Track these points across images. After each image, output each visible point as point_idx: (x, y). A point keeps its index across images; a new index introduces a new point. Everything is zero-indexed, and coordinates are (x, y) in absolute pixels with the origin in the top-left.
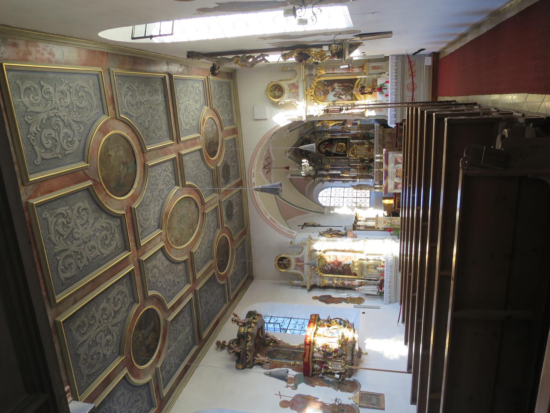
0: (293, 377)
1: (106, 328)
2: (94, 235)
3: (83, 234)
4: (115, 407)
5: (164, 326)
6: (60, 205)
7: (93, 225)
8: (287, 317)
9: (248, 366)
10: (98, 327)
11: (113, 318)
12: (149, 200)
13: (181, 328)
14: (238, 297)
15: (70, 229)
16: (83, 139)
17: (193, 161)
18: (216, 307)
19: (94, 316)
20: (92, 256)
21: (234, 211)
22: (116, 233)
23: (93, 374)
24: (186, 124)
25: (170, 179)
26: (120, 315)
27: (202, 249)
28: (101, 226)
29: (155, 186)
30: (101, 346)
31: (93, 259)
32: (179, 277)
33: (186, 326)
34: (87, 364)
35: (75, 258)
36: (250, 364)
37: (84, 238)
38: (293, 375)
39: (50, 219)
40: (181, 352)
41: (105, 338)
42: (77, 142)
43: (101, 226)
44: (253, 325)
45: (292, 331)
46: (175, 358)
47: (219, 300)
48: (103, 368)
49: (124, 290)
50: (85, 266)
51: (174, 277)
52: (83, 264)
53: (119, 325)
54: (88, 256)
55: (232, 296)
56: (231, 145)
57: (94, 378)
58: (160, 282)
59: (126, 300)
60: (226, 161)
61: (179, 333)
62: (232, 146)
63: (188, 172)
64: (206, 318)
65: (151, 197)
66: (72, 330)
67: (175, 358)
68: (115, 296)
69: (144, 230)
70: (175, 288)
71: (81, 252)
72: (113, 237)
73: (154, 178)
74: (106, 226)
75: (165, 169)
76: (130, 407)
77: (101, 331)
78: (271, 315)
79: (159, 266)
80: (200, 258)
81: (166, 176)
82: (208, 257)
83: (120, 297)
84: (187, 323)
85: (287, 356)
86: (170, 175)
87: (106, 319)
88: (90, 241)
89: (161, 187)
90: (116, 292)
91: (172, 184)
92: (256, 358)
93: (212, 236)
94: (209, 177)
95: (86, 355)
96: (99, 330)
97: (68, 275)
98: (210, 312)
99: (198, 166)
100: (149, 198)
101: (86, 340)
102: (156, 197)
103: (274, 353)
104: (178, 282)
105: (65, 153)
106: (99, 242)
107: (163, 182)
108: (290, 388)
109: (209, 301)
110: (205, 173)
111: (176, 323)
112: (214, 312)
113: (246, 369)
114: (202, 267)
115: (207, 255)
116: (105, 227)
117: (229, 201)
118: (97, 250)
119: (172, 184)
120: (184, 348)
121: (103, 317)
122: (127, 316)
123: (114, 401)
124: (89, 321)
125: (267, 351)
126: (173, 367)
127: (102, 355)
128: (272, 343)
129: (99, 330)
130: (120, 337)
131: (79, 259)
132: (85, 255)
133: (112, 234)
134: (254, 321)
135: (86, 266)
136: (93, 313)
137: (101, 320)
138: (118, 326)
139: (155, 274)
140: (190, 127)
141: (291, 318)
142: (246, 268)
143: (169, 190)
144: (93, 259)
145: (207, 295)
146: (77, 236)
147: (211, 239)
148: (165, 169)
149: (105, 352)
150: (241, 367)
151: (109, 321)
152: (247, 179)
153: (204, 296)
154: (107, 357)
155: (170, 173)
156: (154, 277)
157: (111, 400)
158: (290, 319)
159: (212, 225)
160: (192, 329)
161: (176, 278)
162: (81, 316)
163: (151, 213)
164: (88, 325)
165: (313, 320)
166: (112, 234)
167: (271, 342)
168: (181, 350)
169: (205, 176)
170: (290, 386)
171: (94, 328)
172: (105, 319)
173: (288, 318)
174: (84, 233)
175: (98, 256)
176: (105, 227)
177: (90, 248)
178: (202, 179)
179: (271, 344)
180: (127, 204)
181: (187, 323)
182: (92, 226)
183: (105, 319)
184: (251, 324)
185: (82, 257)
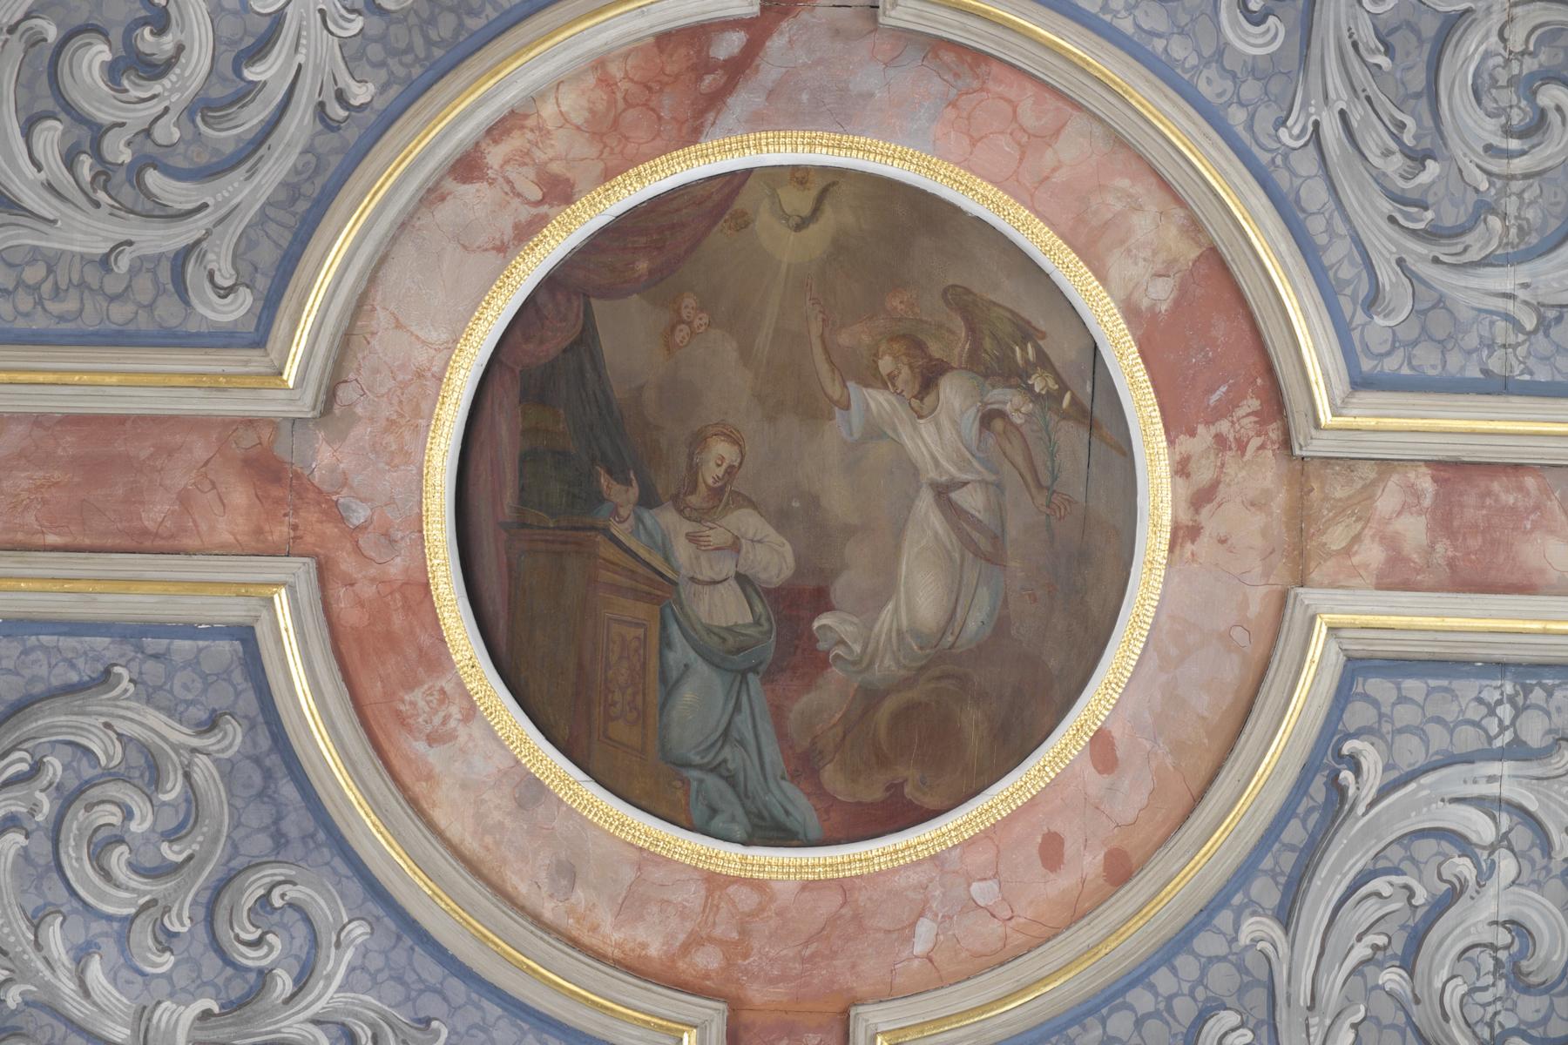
12: (264, 975)
22: (119, 232)
72: (105, 173)
74: (253, 88)
100: (284, 983)
116: (251, 74)
133: (136, 172)
166: (136, 172)
176: (251, 74)
180: (360, 515)
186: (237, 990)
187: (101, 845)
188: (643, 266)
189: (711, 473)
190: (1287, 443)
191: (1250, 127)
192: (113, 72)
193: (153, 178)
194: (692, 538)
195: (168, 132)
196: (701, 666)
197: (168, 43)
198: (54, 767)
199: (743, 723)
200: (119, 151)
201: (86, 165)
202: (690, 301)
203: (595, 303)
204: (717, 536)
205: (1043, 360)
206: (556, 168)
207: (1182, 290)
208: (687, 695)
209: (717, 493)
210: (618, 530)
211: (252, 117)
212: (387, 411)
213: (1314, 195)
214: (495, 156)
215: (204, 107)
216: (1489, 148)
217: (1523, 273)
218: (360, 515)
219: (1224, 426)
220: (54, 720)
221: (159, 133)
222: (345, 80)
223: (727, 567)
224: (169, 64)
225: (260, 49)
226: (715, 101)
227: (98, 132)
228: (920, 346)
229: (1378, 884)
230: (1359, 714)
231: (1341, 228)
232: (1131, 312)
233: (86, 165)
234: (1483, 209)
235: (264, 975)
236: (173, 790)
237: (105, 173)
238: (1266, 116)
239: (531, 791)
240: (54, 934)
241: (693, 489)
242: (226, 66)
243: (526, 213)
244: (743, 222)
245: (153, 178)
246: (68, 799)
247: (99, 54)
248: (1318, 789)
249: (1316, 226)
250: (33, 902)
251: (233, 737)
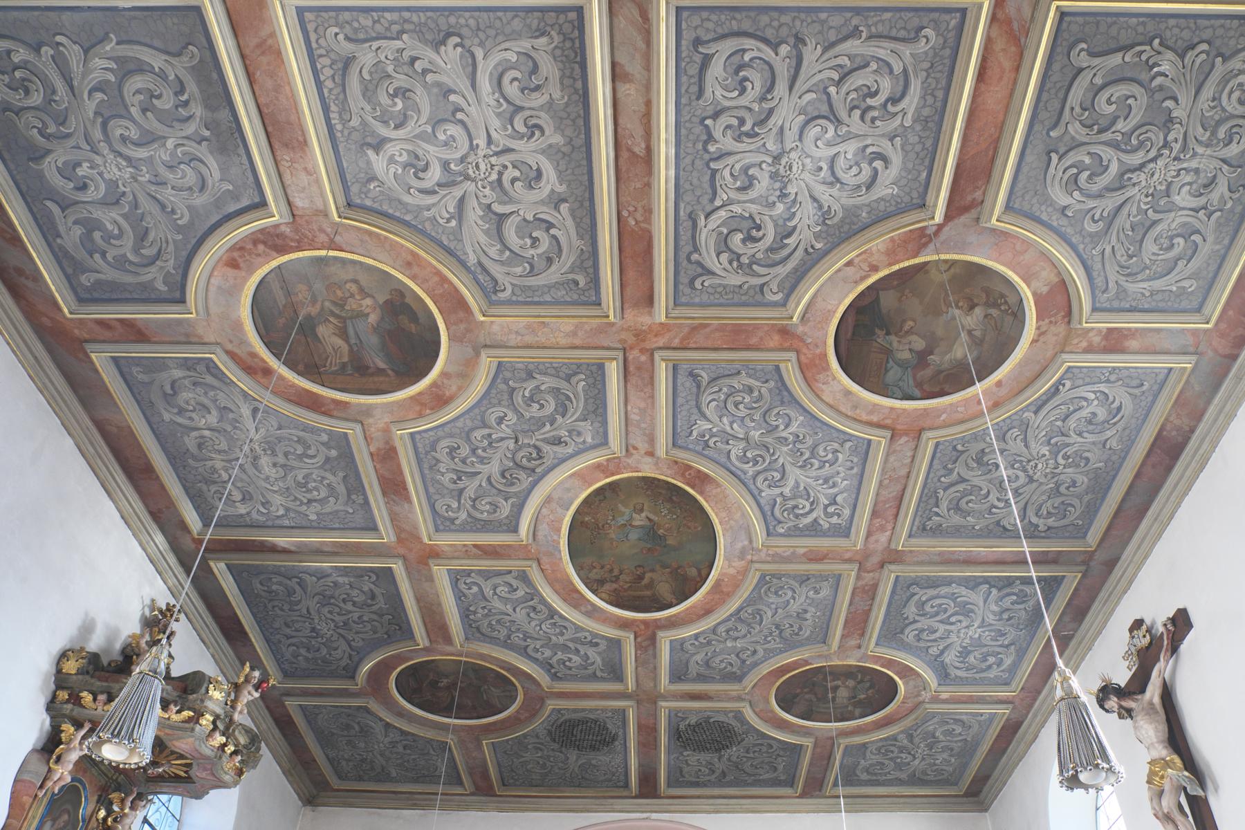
1: (470, 172)
2: (783, 196)
3: (808, 156)
4: (170, 143)
5: (345, 405)
6: (928, 97)
7: (815, 199)
9: (63, 695)
10: (490, 141)
11: (489, 206)
12: (777, 427)
13: (300, 478)
14: (276, 732)
15: (843, 114)
16: (1064, 222)
17: (806, 611)
18: (288, 637)
19: (537, 133)
20: (726, 173)
21: (573, 755)
23: (344, 86)
24: (924, 603)
25: (797, 516)
26: (483, 239)
27: (518, 610)
28: (795, 228)
29: (807, 455)
30: (422, 136)
31: (714, 172)
32: (474, 501)
33: (296, 499)
34: (390, 69)
35: (750, 109)
36: (68, 701)
37: (793, 155)
39: (906, 51)
40: (209, 463)
41: (439, 159)
42: (1063, 199)
43: (795, 228)
44: (219, 739)
46: (207, 433)
47: (308, 650)
48: (339, 127)
49: (553, 268)
50: (710, 138)
51: (489, 479)
52: (717, 134)
53: (453, 223)
54: (730, 160)
55: (291, 704)
56: (781, 767)
57: (329, 84)
58: (500, 420)
59: (518, 270)
60: (743, 740)
61: (283, 466)
62: (776, 769)
63: (782, 588)
64: (274, 587)
65: (784, 434)
66: (536, 37)
67: (207, 433)
68: (553, 231)
69: (699, 387)
70: (446, 479)
71: (757, 135)
72: (740, 266)
73: (830, 456)
74: (786, 245)
75: (835, 503)
76: (136, 205)
77: (473, 148)
79: (555, 426)
80: (495, 593)
81: (812, 504)
82: (478, 628)
83: (540, 251)
84: (302, 503)
86: (808, 520)
87: (499, 180)
88: (774, 176)
89: (794, 474)
90: (563, 240)
91: (780, 522)
93: (538, 656)
94: (729, 668)
95: (425, 72)
96: (481, 141)
97: (717, 69)
98: (286, 607)
99: (780, 633)
100: (782, 427)
101: (474, 85)
102: (773, 454)
103: (66, 817)
104: (461, 491)
105: (1057, 152)
106: (754, 208)
107: (802, 488)
109: (325, 610)
110: (744, 657)
111: (328, 460)
112: (277, 625)
113: (53, 687)
114: (459, 596)
115: (490, 625)
116: (785, 241)
117: (614, 739)
118: (733, 195)
119: (780, 522)
120: (220, 476)
121: (514, 167)
122: (463, 264)
123: (199, 143)
124: (528, 113)
125: (84, 788)
126: (180, 420)
127: (384, 131)
128: (105, 819)
129: (481, 141)
130: (408, 218)
131: (742, 122)
132: (741, 147)
134: (230, 749)
135: (706, 143)
136: (547, 133)
137: (506, 159)
138: (448, 221)
139: (538, 402)
140: (907, 618)
142: (360, 779)
143: (767, 508)
144: (714, 172)
145: (354, 604)
146: (813, 132)
147: (529, 650)
148: (835, 503)
149: (391, 149)
150: (71, 667)
151: (487, 191)
152: (654, 816)
153: (355, 593)
154: (370, 153)
155: (815, 520)
156: (531, 399)
157: (207, 133)
159: (575, 658)
160: (270, 523)
161: (480, 485)
162: (562, 83)
163: (735, 426)
164: (518, 103)
166: (750, 265)
167: (109, 812)
168: (219, 465)
169: (737, 656)
171: (495, 123)
172: (500, 174)
174: (808, 161)
175: (715, 193)
176: (785, 241)
177: (750, 172)
178: (736, 639)
179: (102, 813)
180: (809, 341)
181: (302, 503)
182: (811, 196)
183: (500, 174)
184: (223, 734)
185: (738, 139)
186: (770, 429)
187: (736, 405)
188: (895, 283)
189: (906, 328)
190: (1069, 322)
191: (1084, 250)
192: (744, 241)
193: (755, 267)
194: (899, 342)
195: (760, 256)
196: (895, 366)
197: (761, 234)
198: (725, 390)
199: (905, 378)
200: (745, 260)
201: (735, 264)
202: (907, 291)
203: (880, 292)
204: (904, 341)
205: (1006, 302)
206: (874, 263)
207: (1051, 289)
208: (891, 373)
209: (907, 332)
210: (879, 340)
211: (785, 252)
212: (818, 319)
213: (1098, 266)
214: (856, 261)
215: (771, 249)
216: (1154, 254)
217: (1151, 283)
218: (809, 341)
219: (1053, 319)
220: (727, 381)
221: (757, 256)
222: (814, 242)
223: (907, 347)
224: (760, 239)
225: (789, 235)
226: (925, 245)
227: (739, 256)
228: (972, 300)
229: (1062, 407)
230: (1069, 375)
231: (1102, 274)
232: (1034, 294)
233: (735, 264)
234: (1146, 267)
235: (777, 427)
236: (756, 394)
237: (740, 266)
238: (1090, 246)
239: (848, 393)
240: (725, 420)
241: (901, 331)
242: (778, 239)
243: (864, 274)
244: (927, 272)
245: (755, 267)
246: (728, 396)
247: (740, 236)
248: (1053, 390)
249: (1095, 274)
250: (719, 414)
251: (772, 384)
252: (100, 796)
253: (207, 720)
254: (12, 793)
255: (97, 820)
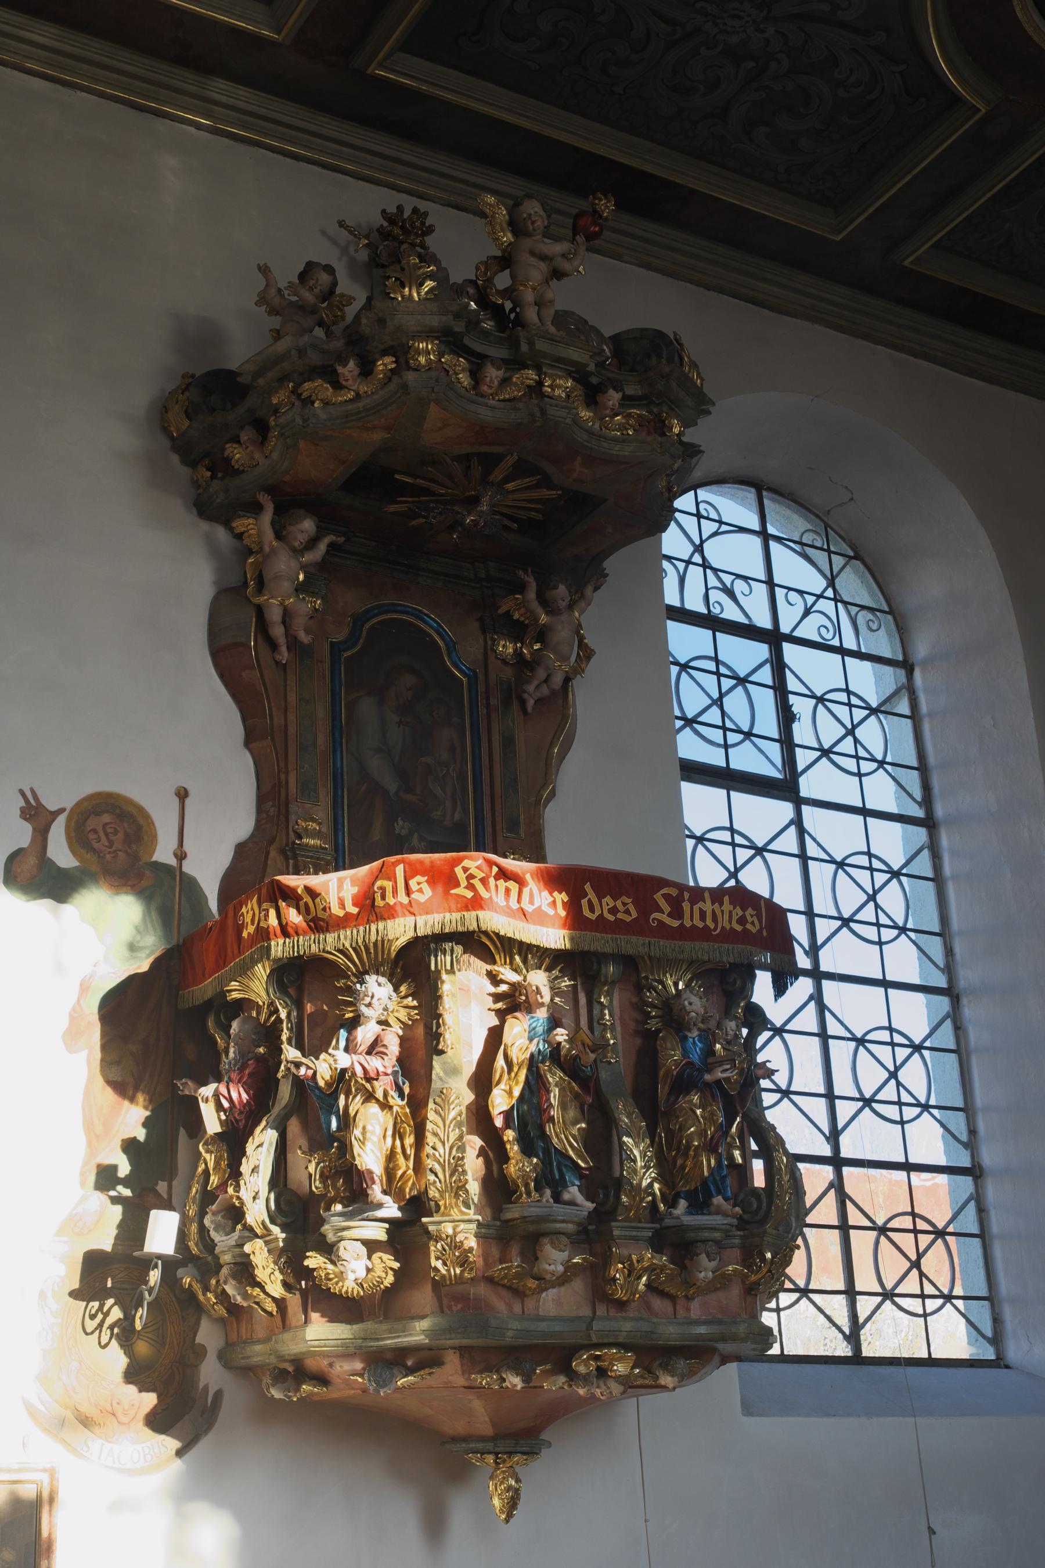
0: (164, 853)
8: (936, 783)
38: (181, 856)
45: (789, 841)
78: (921, 650)
85: (391, 785)
92: (267, 516)
108: (23, 835)
141: (929, 823)
158: (919, 813)
165: (677, 913)
170: (41, 834)
173: (927, 801)
252: (481, 620)
253: (426, 351)
254: (222, 676)
255: (504, 662)
